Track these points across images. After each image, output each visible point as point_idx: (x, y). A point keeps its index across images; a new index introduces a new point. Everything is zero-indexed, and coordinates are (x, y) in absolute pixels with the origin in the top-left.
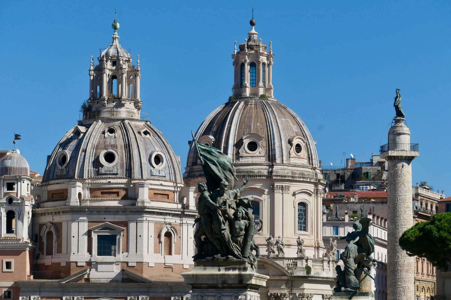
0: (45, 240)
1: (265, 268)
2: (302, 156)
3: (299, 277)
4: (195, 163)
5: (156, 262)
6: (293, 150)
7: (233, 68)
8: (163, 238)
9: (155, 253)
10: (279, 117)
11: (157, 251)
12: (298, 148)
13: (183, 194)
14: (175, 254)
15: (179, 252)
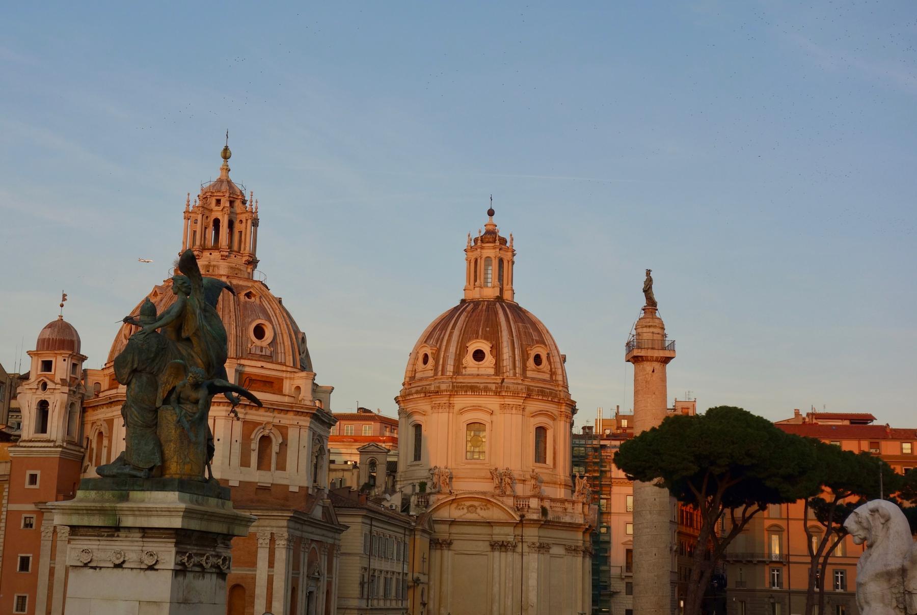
0: (94, 445)
1: (488, 509)
2: (545, 369)
3: (531, 520)
4: (412, 378)
5: (242, 479)
6: (531, 363)
7: (465, 264)
8: (255, 445)
9: (242, 465)
10: (515, 322)
11: (245, 463)
12: (538, 360)
13: (298, 382)
14: (277, 469)
15: (281, 466)
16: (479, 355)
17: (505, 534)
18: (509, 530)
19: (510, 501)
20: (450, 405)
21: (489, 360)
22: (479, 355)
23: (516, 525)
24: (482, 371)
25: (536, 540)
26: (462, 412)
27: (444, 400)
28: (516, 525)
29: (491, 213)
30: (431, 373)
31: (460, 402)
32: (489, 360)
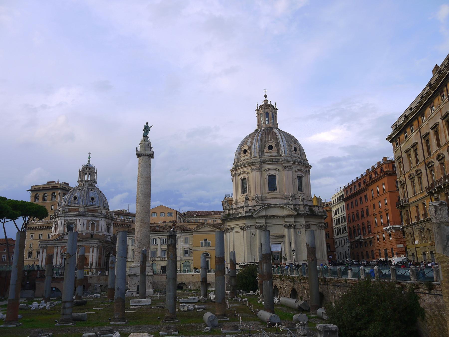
16: (270, 148)
17: (290, 221)
18: (293, 219)
19: (292, 207)
20: (260, 169)
21: (275, 149)
22: (270, 148)
23: (295, 217)
24: (273, 154)
25: (304, 223)
26: (265, 171)
27: (258, 166)
28: (295, 217)
29: (266, 96)
30: (249, 157)
31: (265, 167)
32: (275, 149)
